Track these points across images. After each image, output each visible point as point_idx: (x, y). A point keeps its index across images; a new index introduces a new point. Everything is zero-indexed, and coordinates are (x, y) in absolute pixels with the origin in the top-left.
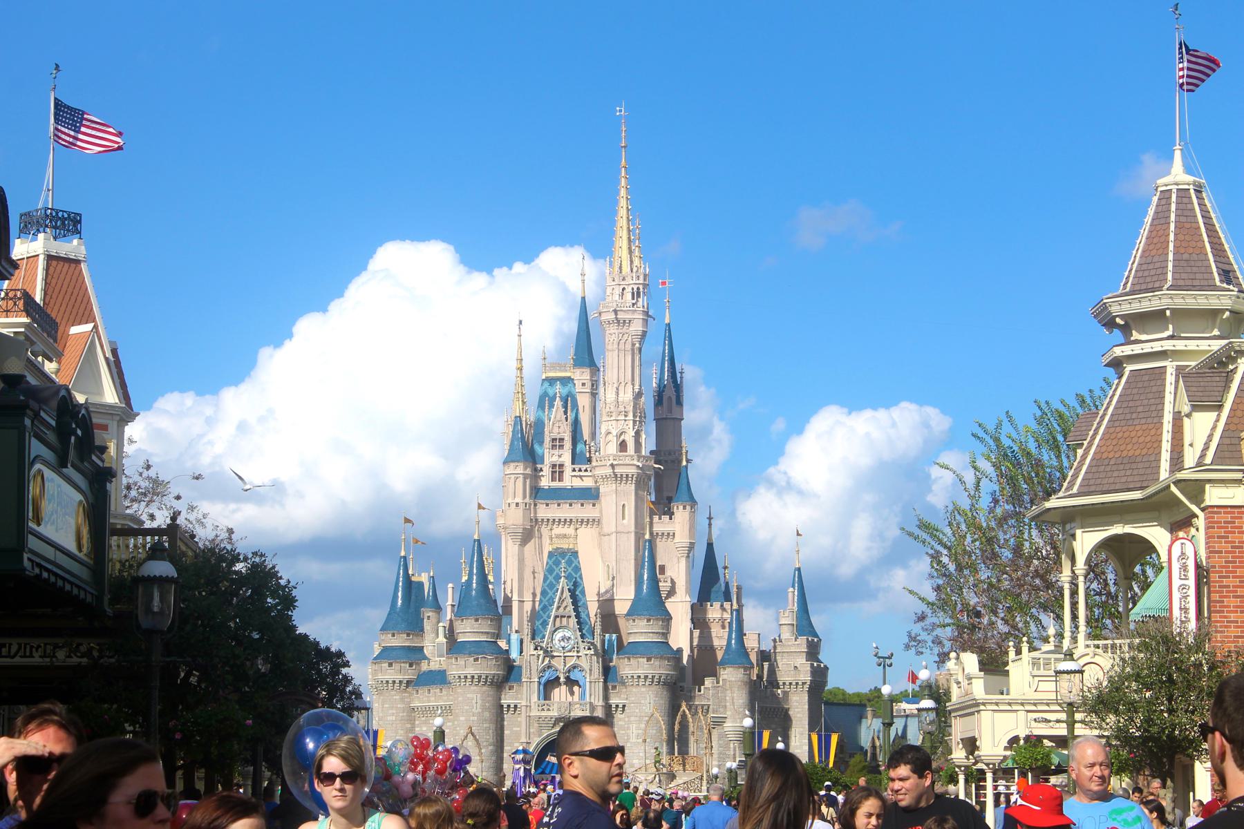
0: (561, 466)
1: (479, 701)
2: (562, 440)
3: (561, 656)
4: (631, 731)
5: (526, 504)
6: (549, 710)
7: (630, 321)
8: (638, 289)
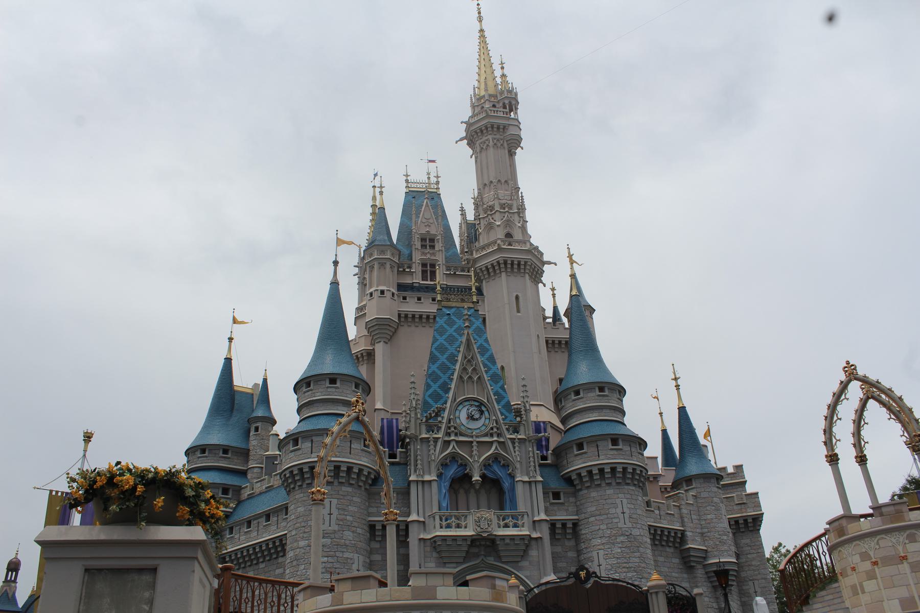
0: (433, 266)
2: (432, 240)
3: (472, 442)
4: (596, 562)
5: (393, 294)
6: (458, 526)
7: (504, 128)
8: (510, 103)
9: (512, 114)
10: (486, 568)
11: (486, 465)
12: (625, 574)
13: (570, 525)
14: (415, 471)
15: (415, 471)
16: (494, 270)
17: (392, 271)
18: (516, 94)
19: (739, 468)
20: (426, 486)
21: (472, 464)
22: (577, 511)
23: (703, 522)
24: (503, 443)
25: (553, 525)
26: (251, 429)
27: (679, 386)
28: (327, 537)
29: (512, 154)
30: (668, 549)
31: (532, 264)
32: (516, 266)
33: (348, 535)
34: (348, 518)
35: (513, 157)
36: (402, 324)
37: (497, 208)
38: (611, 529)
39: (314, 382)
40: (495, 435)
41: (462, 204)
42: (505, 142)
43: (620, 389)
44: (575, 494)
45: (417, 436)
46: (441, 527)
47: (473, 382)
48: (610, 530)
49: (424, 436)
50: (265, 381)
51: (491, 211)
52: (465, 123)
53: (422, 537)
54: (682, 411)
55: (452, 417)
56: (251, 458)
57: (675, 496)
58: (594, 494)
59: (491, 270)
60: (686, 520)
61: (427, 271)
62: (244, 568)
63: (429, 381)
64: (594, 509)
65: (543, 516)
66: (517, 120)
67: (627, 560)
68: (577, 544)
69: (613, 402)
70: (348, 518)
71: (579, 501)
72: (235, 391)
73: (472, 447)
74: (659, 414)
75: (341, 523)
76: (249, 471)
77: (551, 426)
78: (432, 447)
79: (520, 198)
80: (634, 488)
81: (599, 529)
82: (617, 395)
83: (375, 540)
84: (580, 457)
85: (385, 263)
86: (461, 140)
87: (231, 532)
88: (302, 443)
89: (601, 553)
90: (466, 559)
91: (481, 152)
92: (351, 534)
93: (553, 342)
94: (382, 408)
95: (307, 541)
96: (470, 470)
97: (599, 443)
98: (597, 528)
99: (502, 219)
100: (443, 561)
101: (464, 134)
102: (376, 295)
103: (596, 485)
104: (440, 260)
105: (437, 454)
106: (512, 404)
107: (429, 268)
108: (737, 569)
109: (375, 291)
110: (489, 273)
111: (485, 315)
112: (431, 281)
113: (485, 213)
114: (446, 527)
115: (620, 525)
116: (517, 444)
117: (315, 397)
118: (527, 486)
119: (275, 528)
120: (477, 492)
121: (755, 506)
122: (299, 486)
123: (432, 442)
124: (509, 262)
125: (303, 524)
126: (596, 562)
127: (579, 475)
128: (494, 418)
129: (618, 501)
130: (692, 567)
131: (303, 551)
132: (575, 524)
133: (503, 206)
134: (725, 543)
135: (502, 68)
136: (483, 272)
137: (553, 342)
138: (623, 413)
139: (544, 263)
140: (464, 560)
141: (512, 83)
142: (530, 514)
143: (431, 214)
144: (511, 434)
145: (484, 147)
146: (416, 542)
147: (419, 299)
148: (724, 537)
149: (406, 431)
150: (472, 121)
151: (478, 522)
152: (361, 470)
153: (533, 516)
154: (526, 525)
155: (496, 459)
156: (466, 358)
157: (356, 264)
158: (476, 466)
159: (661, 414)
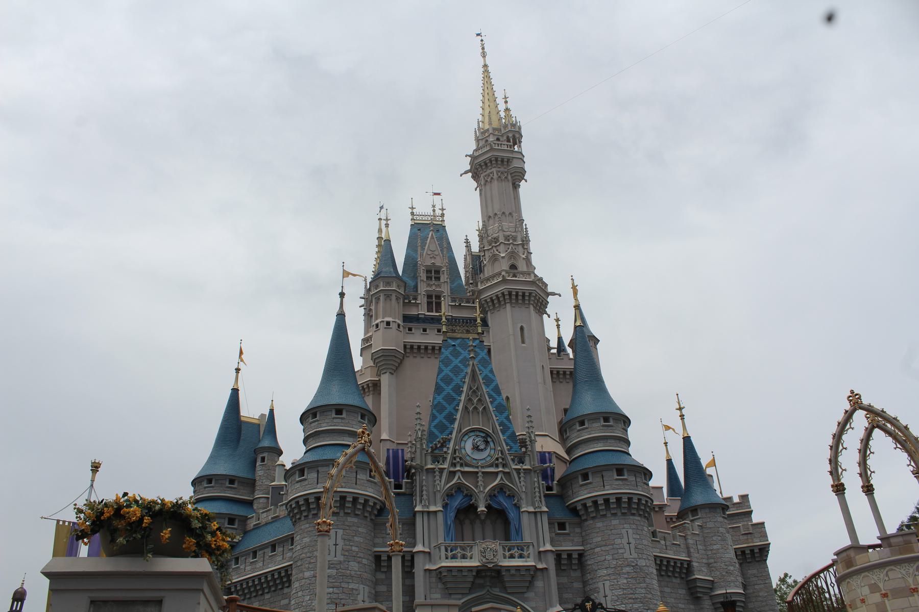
0: (438, 297)
1: (340, 542)
2: (437, 272)
3: (477, 473)
5: (399, 325)
6: (464, 557)
7: (508, 161)
8: (514, 136)
9: (516, 147)
10: (490, 598)
11: (492, 496)
12: (631, 605)
13: (575, 556)
14: (421, 502)
15: (421, 502)
16: (499, 302)
17: (398, 303)
18: (520, 128)
19: (744, 498)
20: (432, 517)
21: (477, 495)
22: (583, 541)
23: (710, 553)
24: (509, 473)
25: (558, 556)
26: (258, 460)
27: (684, 415)
28: (332, 568)
29: (516, 187)
30: (674, 580)
31: (536, 295)
32: (520, 298)
33: (354, 566)
34: (354, 548)
35: (517, 190)
36: (408, 355)
37: (501, 240)
38: (616, 559)
39: (320, 413)
40: (500, 466)
41: (466, 236)
42: (509, 175)
43: (624, 419)
44: (581, 524)
45: (423, 467)
46: (447, 558)
47: (478, 413)
48: (615, 560)
49: (430, 466)
50: (272, 411)
51: (496, 243)
52: (469, 156)
53: (427, 567)
54: (687, 441)
55: (457, 447)
56: (257, 488)
57: (681, 526)
58: (599, 525)
59: (496, 302)
60: (692, 550)
61: (432, 303)
62: (249, 598)
63: (434, 411)
64: (599, 539)
65: (548, 547)
66: (521, 153)
67: (634, 591)
68: (583, 575)
69: (617, 432)
70: (354, 548)
71: (585, 531)
72: (241, 422)
73: (478, 477)
74: (664, 443)
75: (347, 553)
76: (255, 502)
77: (556, 456)
78: (438, 477)
79: (525, 230)
80: (639, 518)
81: (605, 559)
82: (621, 425)
83: (380, 571)
84: (585, 487)
85: (391, 295)
86: (466, 172)
87: (237, 563)
88: (308, 473)
89: (607, 583)
90: (471, 590)
91: (485, 184)
92: (357, 565)
93: (558, 372)
94: (388, 438)
95: (312, 572)
96: (475, 501)
97: (604, 473)
98: (603, 558)
99: (507, 251)
100: (448, 592)
101: (469, 168)
102: (382, 326)
103: (601, 515)
104: (446, 292)
105: (443, 484)
106: (517, 434)
107: (434, 299)
108: (744, 600)
109: (381, 322)
110: (494, 304)
111: (490, 346)
112: (436, 312)
113: (490, 245)
114: (452, 558)
115: (626, 556)
116: (522, 475)
117: (321, 427)
118: (533, 516)
119: (280, 558)
120: (483, 523)
121: (761, 536)
122: (305, 516)
123: (437, 473)
125: (308, 555)
126: (602, 593)
127: (585, 505)
128: (499, 448)
129: (624, 531)
130: (698, 598)
131: (308, 582)
132: (581, 555)
133: (507, 238)
134: (732, 574)
135: (506, 102)
136: (487, 303)
137: (558, 372)
138: (628, 443)
139: (548, 294)
140: (469, 591)
141: (516, 117)
142: (535, 544)
143: (437, 247)
144: (516, 465)
145: (489, 180)
146: (422, 573)
147: (425, 330)
148: (730, 567)
149: (412, 461)
150: (477, 154)
151: (483, 553)
152: (366, 501)
153: (539, 547)
154: (531, 556)
155: (501, 489)
156: (471, 388)
157: (363, 296)
158: (482, 496)
159: (666, 444)
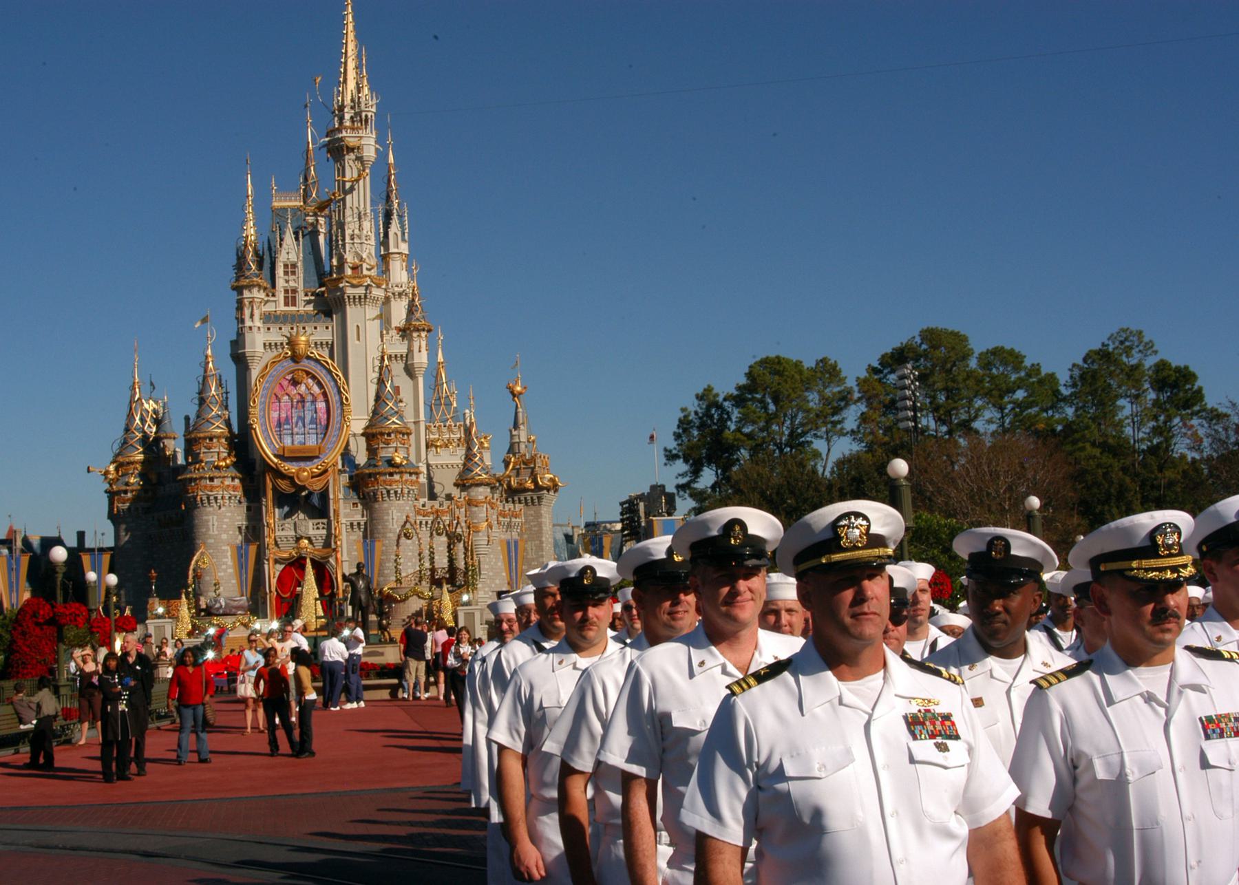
0: (294, 291)
2: (294, 266)
8: (366, 116)
61: (288, 297)
124: (351, 297)
129: (390, 512)
